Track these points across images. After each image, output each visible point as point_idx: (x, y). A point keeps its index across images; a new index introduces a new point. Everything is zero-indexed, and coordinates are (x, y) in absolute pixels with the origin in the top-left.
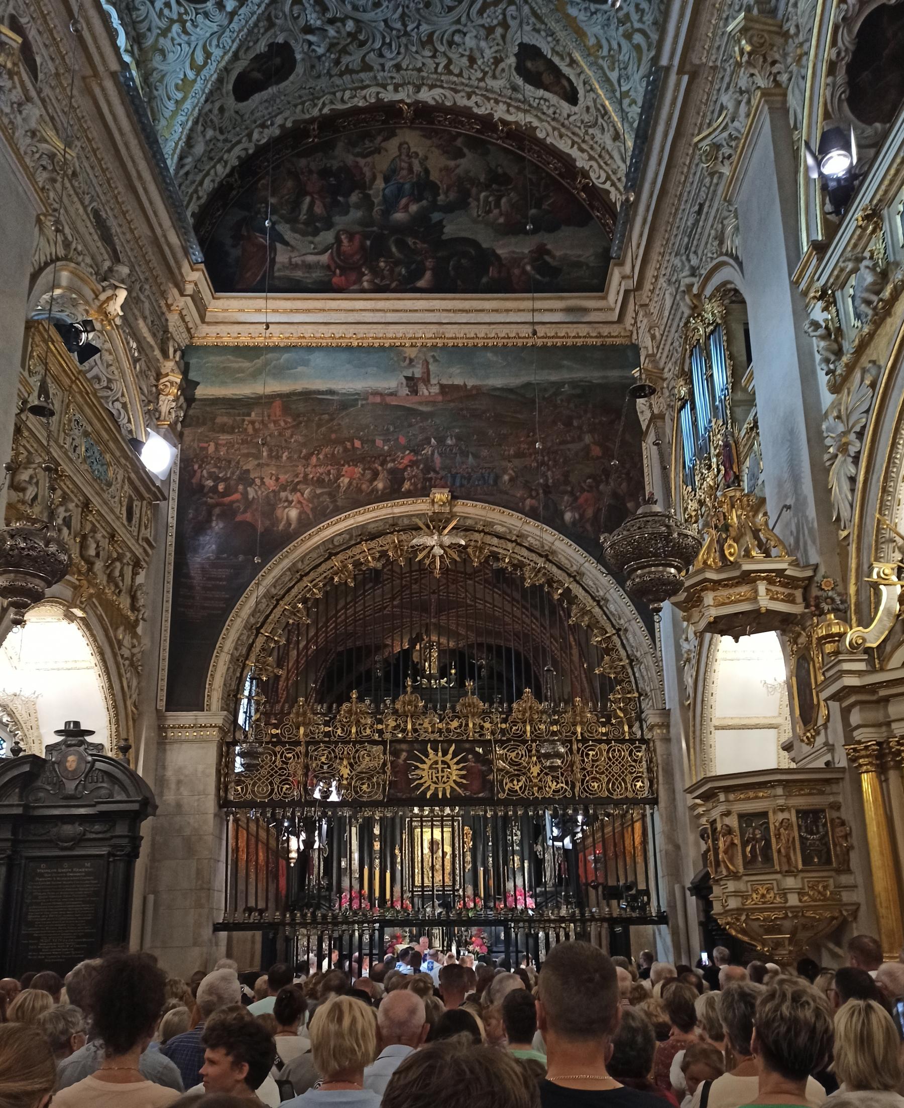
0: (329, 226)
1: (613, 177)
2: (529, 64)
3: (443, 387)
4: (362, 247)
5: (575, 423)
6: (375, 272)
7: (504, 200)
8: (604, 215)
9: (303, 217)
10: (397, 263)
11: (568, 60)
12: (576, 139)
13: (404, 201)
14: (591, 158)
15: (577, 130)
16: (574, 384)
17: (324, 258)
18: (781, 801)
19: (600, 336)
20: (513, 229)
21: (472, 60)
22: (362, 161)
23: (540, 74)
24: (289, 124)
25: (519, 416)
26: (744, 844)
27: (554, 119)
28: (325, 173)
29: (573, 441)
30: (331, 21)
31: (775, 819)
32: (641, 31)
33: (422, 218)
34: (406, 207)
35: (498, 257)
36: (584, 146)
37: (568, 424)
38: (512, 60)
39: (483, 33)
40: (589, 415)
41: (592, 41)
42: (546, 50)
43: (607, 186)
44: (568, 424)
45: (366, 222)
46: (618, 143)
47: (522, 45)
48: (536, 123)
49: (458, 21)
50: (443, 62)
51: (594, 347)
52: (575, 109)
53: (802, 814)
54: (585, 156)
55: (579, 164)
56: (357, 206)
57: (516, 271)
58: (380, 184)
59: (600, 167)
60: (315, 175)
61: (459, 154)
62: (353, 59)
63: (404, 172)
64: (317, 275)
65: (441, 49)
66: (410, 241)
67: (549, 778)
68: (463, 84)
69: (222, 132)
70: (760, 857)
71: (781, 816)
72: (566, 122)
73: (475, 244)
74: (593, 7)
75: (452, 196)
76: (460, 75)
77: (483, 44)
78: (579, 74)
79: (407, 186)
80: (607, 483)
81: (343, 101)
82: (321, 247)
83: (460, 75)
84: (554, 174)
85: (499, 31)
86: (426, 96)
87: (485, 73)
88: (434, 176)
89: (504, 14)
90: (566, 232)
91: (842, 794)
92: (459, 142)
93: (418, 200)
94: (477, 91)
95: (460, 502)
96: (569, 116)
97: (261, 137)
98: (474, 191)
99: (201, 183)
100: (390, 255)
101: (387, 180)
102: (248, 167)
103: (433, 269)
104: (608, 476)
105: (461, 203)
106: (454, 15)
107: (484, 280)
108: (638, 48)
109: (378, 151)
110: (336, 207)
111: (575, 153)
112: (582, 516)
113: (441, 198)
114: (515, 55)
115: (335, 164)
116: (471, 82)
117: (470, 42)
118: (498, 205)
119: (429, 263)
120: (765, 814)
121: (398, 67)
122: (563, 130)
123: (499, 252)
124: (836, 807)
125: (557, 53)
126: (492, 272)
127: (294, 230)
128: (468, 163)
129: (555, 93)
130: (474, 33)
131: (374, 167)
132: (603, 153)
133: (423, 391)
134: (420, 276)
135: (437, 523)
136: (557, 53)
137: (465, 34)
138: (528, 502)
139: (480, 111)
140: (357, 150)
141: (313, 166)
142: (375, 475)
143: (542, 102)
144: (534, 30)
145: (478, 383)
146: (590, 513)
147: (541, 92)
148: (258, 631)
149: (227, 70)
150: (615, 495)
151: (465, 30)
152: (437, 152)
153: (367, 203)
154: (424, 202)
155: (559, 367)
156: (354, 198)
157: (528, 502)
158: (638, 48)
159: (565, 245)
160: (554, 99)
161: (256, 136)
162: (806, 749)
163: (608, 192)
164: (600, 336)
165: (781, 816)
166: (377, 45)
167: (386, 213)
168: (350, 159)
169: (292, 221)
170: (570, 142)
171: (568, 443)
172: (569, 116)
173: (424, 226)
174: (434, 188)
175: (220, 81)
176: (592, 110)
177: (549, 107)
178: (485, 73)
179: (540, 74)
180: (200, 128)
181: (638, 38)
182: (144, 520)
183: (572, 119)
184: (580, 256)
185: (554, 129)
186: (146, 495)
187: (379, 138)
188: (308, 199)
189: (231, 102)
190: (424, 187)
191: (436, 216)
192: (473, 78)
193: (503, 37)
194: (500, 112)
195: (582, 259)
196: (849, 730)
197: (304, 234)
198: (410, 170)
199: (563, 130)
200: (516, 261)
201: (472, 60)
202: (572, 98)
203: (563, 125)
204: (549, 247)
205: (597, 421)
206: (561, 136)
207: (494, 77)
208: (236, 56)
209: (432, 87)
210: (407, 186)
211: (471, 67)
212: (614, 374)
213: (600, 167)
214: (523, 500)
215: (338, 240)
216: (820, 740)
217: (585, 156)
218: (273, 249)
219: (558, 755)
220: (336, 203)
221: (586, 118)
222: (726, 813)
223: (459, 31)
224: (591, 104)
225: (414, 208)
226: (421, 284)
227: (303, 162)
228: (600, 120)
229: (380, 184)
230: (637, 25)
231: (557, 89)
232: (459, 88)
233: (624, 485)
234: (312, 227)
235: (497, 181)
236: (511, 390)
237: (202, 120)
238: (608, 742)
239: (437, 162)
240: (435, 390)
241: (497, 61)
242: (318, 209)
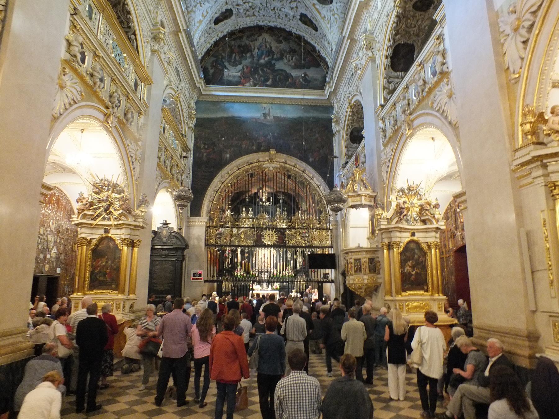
0: (241, 63)
3: (274, 117)
4: (251, 70)
6: (254, 79)
7: (294, 58)
9: (233, 60)
10: (261, 76)
13: (263, 56)
16: (314, 118)
17: (239, 74)
18: (365, 256)
20: (297, 66)
21: (286, 16)
22: (251, 43)
26: (355, 267)
28: (239, 46)
31: (363, 261)
32: (338, 14)
33: (269, 62)
34: (264, 58)
35: (292, 76)
38: (299, 17)
41: (323, 15)
42: (309, 16)
45: (252, 63)
47: (301, 14)
48: (305, 35)
50: (278, 15)
53: (370, 259)
55: (317, 49)
56: (250, 58)
57: (297, 81)
58: (256, 50)
60: (236, 47)
61: (281, 42)
63: (264, 47)
64: (236, 79)
66: (265, 69)
70: (359, 270)
71: (364, 260)
73: (285, 71)
74: (323, 6)
75: (278, 55)
79: (265, 52)
82: (238, 70)
83: (282, 19)
84: (310, 50)
85: (295, 9)
86: (272, 24)
87: (290, 19)
88: (273, 49)
90: (313, 69)
91: (379, 254)
92: (281, 38)
93: (268, 56)
95: (279, 154)
98: (285, 54)
100: (259, 74)
101: (259, 49)
103: (272, 79)
105: (281, 58)
106: (282, 3)
107: (287, 83)
108: (336, 18)
109: (256, 40)
110: (242, 57)
111: (316, 45)
112: (315, 159)
113: (275, 56)
115: (243, 44)
118: (292, 59)
119: (271, 77)
120: (360, 259)
121: (264, 16)
123: (292, 74)
124: (378, 257)
126: (290, 80)
127: (229, 64)
128: (284, 46)
131: (254, 45)
133: (268, 118)
134: (268, 80)
135: (271, 161)
139: (288, 30)
140: (250, 39)
141: (236, 44)
142: (253, 145)
145: (285, 116)
147: (307, 27)
148: (217, 192)
152: (274, 41)
153: (252, 56)
154: (270, 57)
156: (248, 55)
157: (299, 154)
158: (336, 18)
159: (312, 73)
160: (310, 29)
162: (372, 241)
165: (364, 260)
166: (257, 10)
167: (258, 60)
168: (247, 42)
169: (229, 61)
173: (269, 65)
174: (273, 53)
181: (336, 16)
187: (257, 36)
188: (234, 55)
190: (270, 52)
191: (273, 62)
194: (294, 31)
196: (382, 239)
197: (233, 66)
198: (266, 47)
200: (297, 77)
202: (316, 30)
204: (307, 73)
209: (273, 22)
210: (265, 52)
215: (243, 69)
216: (376, 239)
218: (223, 70)
219: (306, 237)
220: (243, 56)
222: (352, 258)
225: (267, 59)
226: (268, 83)
227: (233, 43)
229: (256, 50)
230: (336, 12)
234: (235, 64)
235: (292, 51)
236: (295, 119)
238: (320, 229)
239: (274, 45)
240: (272, 118)
241: (294, 17)
242: (237, 58)
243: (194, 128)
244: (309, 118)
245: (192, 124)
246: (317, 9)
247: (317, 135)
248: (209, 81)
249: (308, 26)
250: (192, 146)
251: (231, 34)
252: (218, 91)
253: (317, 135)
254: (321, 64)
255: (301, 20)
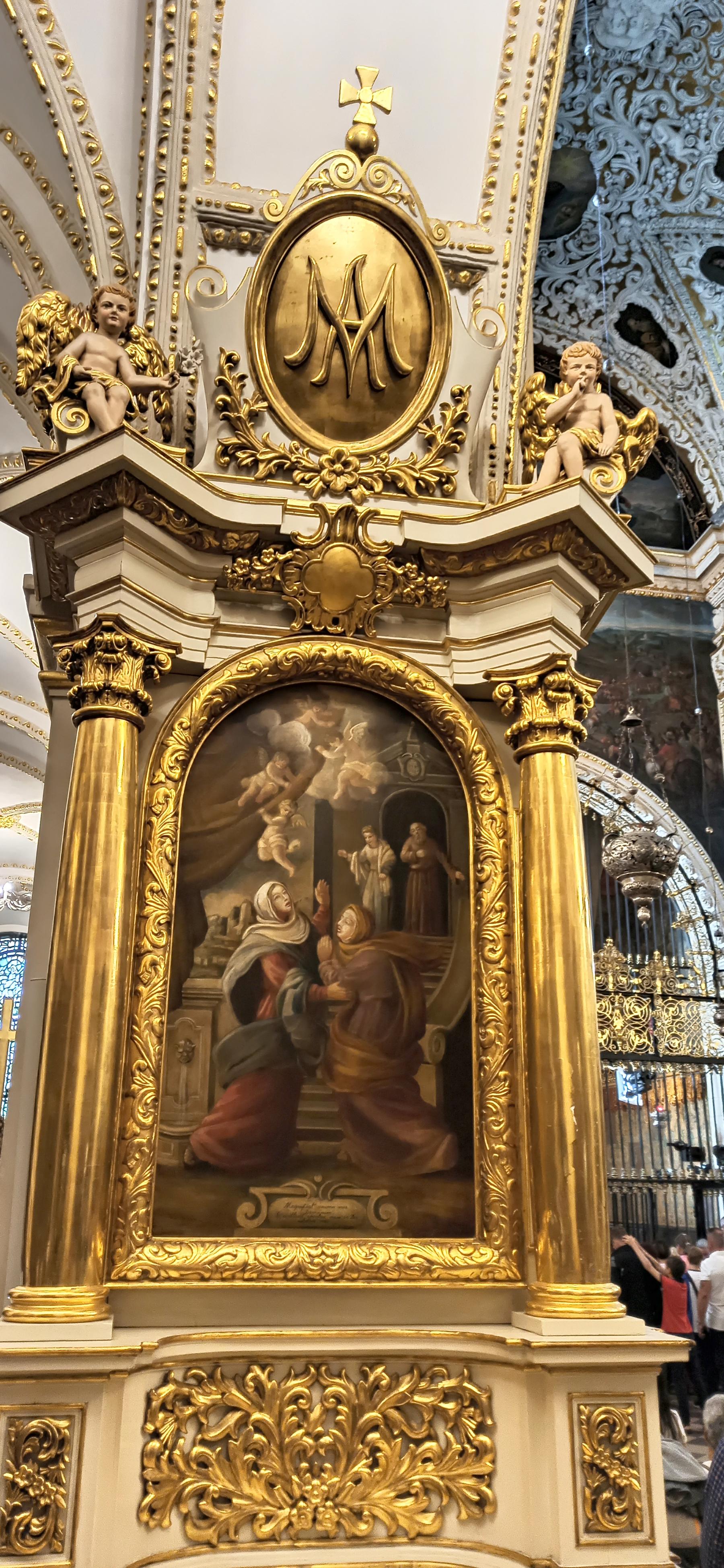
1: (696, 439)
2: (632, 323)
5: (655, 674)
8: (676, 472)
11: (678, 328)
12: (661, 397)
14: (675, 418)
15: (663, 389)
16: (653, 635)
19: (676, 590)
21: (573, 308)
23: (640, 333)
25: (602, 661)
27: (641, 375)
29: (653, 692)
36: (669, 406)
37: (648, 674)
38: (615, 316)
39: (595, 287)
40: (667, 667)
41: (709, 317)
43: (688, 446)
44: (648, 674)
46: (711, 410)
48: (621, 374)
49: (575, 273)
50: (543, 303)
51: (669, 600)
52: (667, 370)
54: (669, 415)
59: (683, 428)
65: (546, 292)
67: (632, 1032)
68: (556, 327)
72: (653, 380)
76: (556, 318)
77: (592, 297)
78: (686, 343)
80: (687, 738)
85: (613, 289)
87: (581, 321)
89: (625, 277)
94: (569, 336)
96: (658, 375)
104: (687, 730)
114: (621, 313)
116: (564, 327)
117: (580, 292)
122: (649, 387)
125: (669, 320)
129: (651, 353)
130: (587, 285)
132: (688, 415)
136: (669, 320)
137: (576, 285)
138: (611, 748)
143: (633, 357)
144: (652, 296)
146: (670, 765)
147: (635, 349)
150: (694, 750)
151: (578, 281)
155: (638, 616)
157: (611, 748)
160: (647, 357)
163: (686, 452)
164: (676, 590)
170: (654, 399)
171: (647, 692)
172: (658, 375)
176: (689, 375)
177: (639, 364)
178: (581, 321)
179: (640, 333)
183: (660, 378)
184: (653, 508)
185: (639, 384)
192: (567, 323)
193: (615, 295)
195: (654, 511)
199: (649, 387)
201: (573, 308)
202: (669, 359)
203: (650, 383)
205: (675, 674)
206: (645, 392)
207: (589, 326)
211: (569, 313)
212: (689, 630)
213: (683, 428)
214: (607, 746)
217: (669, 415)
221: (678, 381)
223: (571, 281)
224: (690, 371)
228: (695, 385)
231: (655, 349)
232: (551, 330)
233: (702, 741)
244: (637, 635)
246: (695, 296)
247: (667, 691)
249: (642, 347)
253: (667, 691)
254: (667, 468)
255: (621, 327)
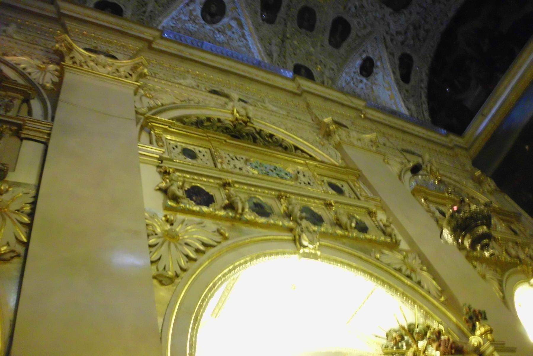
24: (427, 71)
30: (406, 33)
62: (422, 33)
69: (413, 96)
81: (432, 47)
97: (424, 85)
99: (424, 115)
102: (431, 97)
149: (396, 79)
161: (423, 85)
166: (423, 22)
175: (398, 84)
180: (406, 102)
182: (522, 229)
186: (513, 220)
189: (407, 86)
208: (394, 73)
237: (406, 100)
243: (498, 189)
245: (490, 184)
248: (459, 131)
250: (516, 206)
251: (433, 72)
252: (482, 125)
